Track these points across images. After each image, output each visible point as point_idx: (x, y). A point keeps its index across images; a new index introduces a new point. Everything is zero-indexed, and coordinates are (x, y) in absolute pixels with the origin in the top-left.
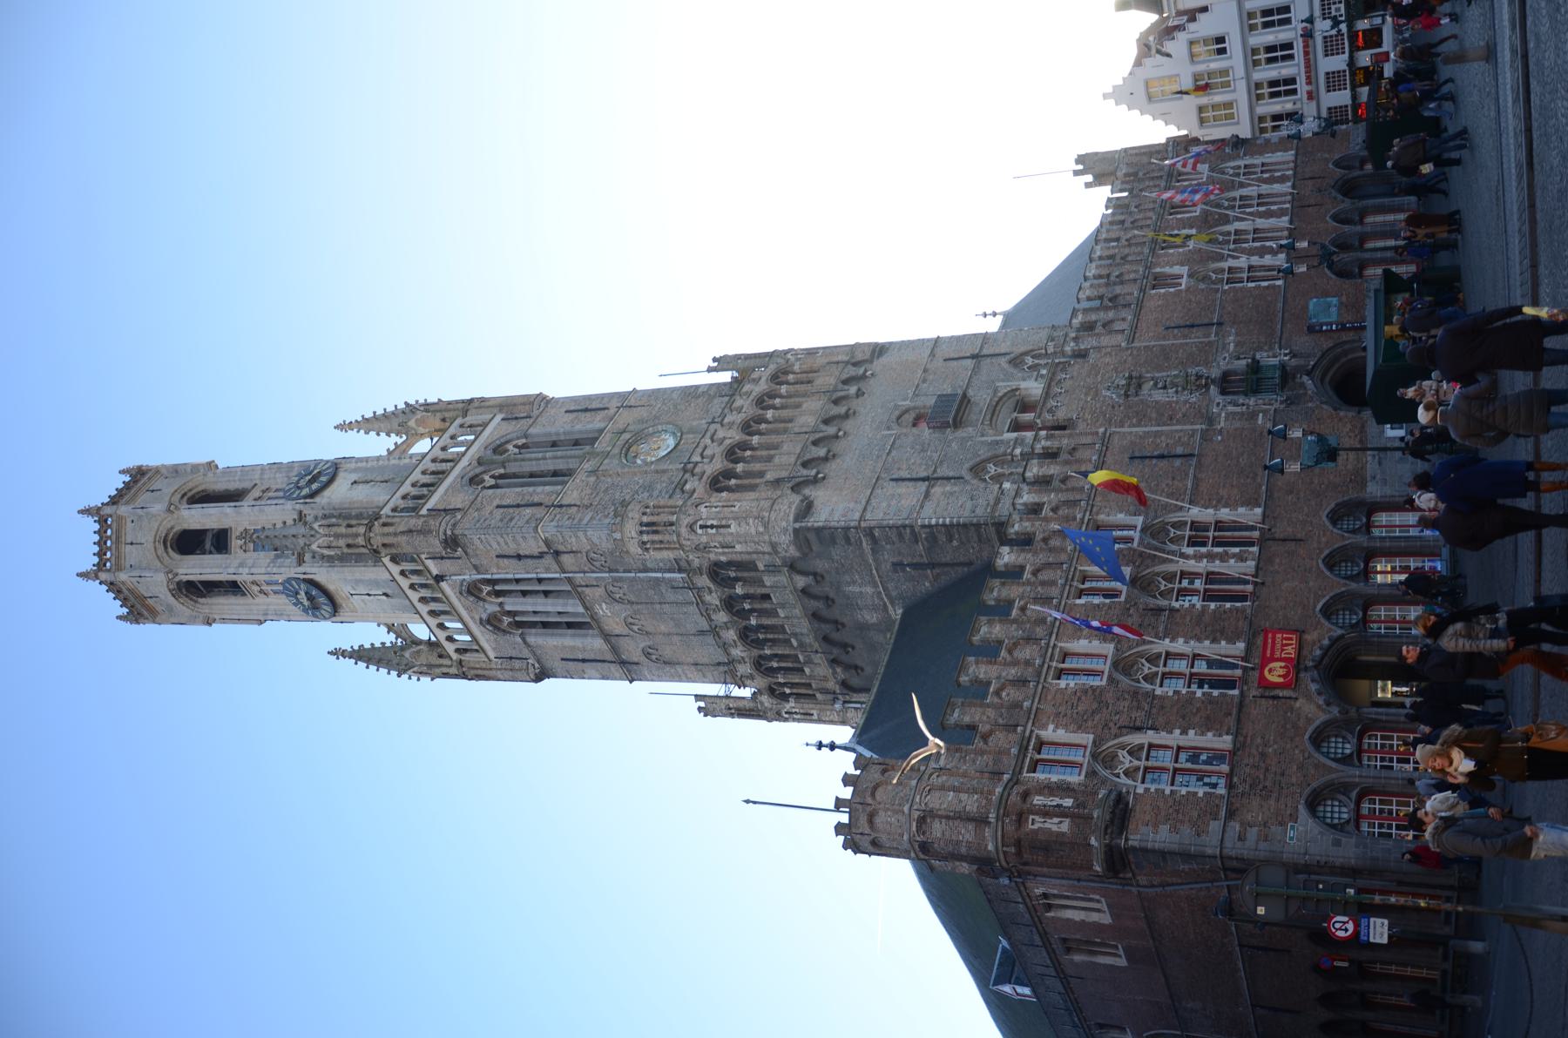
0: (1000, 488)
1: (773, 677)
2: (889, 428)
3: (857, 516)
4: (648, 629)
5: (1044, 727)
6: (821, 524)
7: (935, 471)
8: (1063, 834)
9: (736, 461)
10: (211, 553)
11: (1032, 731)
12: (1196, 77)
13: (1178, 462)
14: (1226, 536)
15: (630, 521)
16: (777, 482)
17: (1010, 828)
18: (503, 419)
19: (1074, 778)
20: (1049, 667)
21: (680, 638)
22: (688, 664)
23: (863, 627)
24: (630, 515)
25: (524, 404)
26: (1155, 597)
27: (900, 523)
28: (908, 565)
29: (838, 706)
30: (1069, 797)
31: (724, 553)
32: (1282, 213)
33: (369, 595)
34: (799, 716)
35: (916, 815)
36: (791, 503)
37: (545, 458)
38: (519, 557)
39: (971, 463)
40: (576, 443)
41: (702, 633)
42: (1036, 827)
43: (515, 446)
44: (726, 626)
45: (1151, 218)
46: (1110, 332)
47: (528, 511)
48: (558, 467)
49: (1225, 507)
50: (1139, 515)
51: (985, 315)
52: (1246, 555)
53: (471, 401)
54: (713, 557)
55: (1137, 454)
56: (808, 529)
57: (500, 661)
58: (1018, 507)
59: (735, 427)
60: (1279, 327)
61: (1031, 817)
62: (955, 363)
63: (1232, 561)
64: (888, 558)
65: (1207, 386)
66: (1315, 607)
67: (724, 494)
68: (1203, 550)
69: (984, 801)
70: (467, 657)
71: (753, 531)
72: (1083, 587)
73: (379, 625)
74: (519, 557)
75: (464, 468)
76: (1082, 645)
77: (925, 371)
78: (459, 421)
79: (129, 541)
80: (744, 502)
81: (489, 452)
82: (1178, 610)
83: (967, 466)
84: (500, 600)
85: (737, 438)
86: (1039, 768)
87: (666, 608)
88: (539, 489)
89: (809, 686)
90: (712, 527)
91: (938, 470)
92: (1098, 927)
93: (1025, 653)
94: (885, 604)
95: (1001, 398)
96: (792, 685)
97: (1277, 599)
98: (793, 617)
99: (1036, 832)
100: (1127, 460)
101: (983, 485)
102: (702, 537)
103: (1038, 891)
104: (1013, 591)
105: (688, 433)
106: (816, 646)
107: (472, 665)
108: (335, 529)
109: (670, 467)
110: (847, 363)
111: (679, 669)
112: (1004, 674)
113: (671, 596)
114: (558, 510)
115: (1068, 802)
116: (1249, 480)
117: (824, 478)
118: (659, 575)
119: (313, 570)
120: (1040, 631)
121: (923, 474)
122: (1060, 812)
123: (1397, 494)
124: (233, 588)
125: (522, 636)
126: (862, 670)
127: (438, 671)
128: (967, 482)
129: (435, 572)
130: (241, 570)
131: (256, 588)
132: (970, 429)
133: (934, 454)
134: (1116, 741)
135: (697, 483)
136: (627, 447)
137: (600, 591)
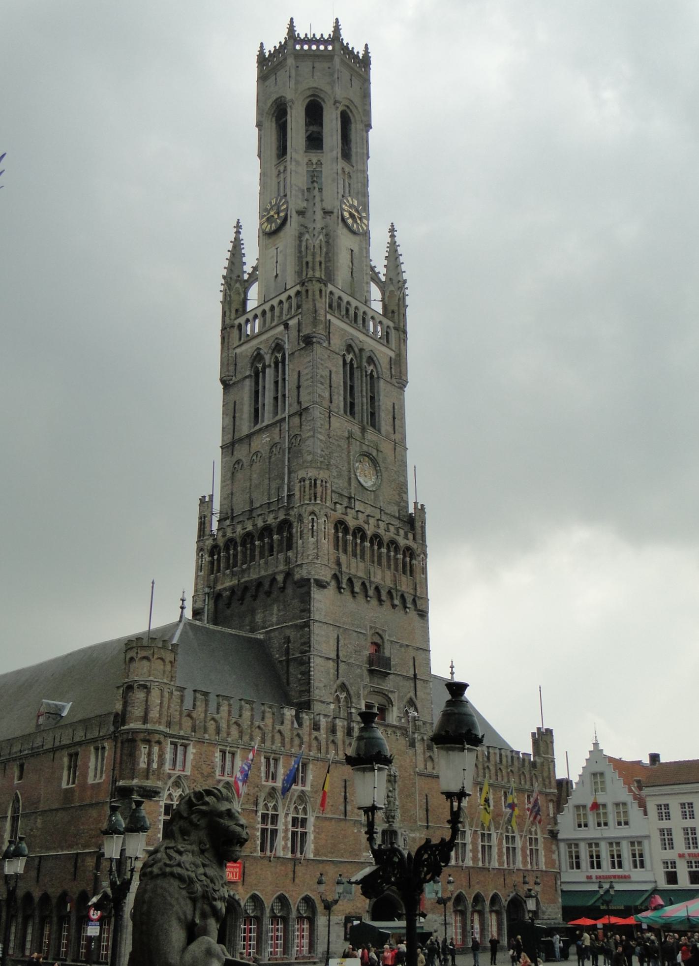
0: (331, 703)
1: (224, 549)
2: (371, 628)
3: (317, 618)
4: (254, 465)
5: (194, 747)
6: (312, 595)
8: (138, 764)
9: (354, 536)
10: (307, 131)
11: (192, 741)
12: (604, 806)
13: (342, 808)
14: (298, 840)
15: (318, 473)
16: (339, 564)
17: (141, 736)
18: (391, 358)
19: (167, 767)
20: (227, 746)
21: (248, 487)
22: (232, 489)
23: (253, 612)
24: (321, 472)
25: (400, 372)
26: (264, 800)
27: (312, 644)
28: (288, 646)
29: (207, 590)
30: (158, 765)
31: (297, 532)
32: (501, 863)
33: (277, 262)
34: (200, 563)
35: (148, 684)
36: (325, 576)
37: (362, 396)
38: (299, 387)
39: (347, 683)
40: (373, 414)
41: (252, 502)
42: (143, 749)
43: (372, 371)
44: (254, 525)
45: (502, 780)
46: (425, 761)
47: (327, 394)
48: (356, 406)
49: (315, 837)
50: (311, 788)
51: (452, 667)
52: (286, 850)
53: (405, 332)
54: (295, 524)
55: (347, 783)
56: (310, 588)
57: (234, 356)
58: (318, 717)
61: (147, 746)
62: (411, 663)
63: (283, 843)
64: (291, 633)
65: (388, 822)
66: (256, 890)
67: (333, 531)
68: (290, 826)
69: (155, 720)
70: (236, 332)
71: (309, 553)
72: (271, 760)
73: (257, 259)
74: (299, 387)
75: (358, 338)
76: (239, 763)
77: (407, 646)
78: (391, 324)
79: (317, 65)
80: (327, 545)
81: (368, 354)
82: (256, 815)
84: (273, 365)
86: (173, 746)
87: (266, 481)
88: (342, 398)
89: (219, 571)
90: (313, 526)
91: (343, 663)
92: (85, 776)
93: (234, 731)
94: (267, 628)
95: (387, 696)
96: (219, 560)
97: (261, 869)
98: (259, 570)
99: (140, 750)
100: (344, 778)
101: (333, 691)
102: (307, 519)
103: (106, 745)
104: (269, 721)
106: (243, 581)
107: (231, 335)
108: (317, 250)
109: (352, 488)
110: (415, 596)
111: (229, 482)
112: (223, 721)
113: (274, 485)
114: (327, 415)
115: (155, 766)
116: (329, 849)
117: (340, 592)
118: (286, 482)
119: (293, 224)
120: (246, 738)
121: (341, 654)
122: (150, 762)
123: (318, 933)
124: (282, 150)
125: (250, 376)
126: (228, 608)
127: (227, 309)
128: (335, 682)
129: (291, 323)
130: (294, 163)
131: (282, 168)
132: (368, 680)
133: (353, 659)
134: (186, 787)
135: (340, 512)
136: (367, 455)
137: (277, 439)
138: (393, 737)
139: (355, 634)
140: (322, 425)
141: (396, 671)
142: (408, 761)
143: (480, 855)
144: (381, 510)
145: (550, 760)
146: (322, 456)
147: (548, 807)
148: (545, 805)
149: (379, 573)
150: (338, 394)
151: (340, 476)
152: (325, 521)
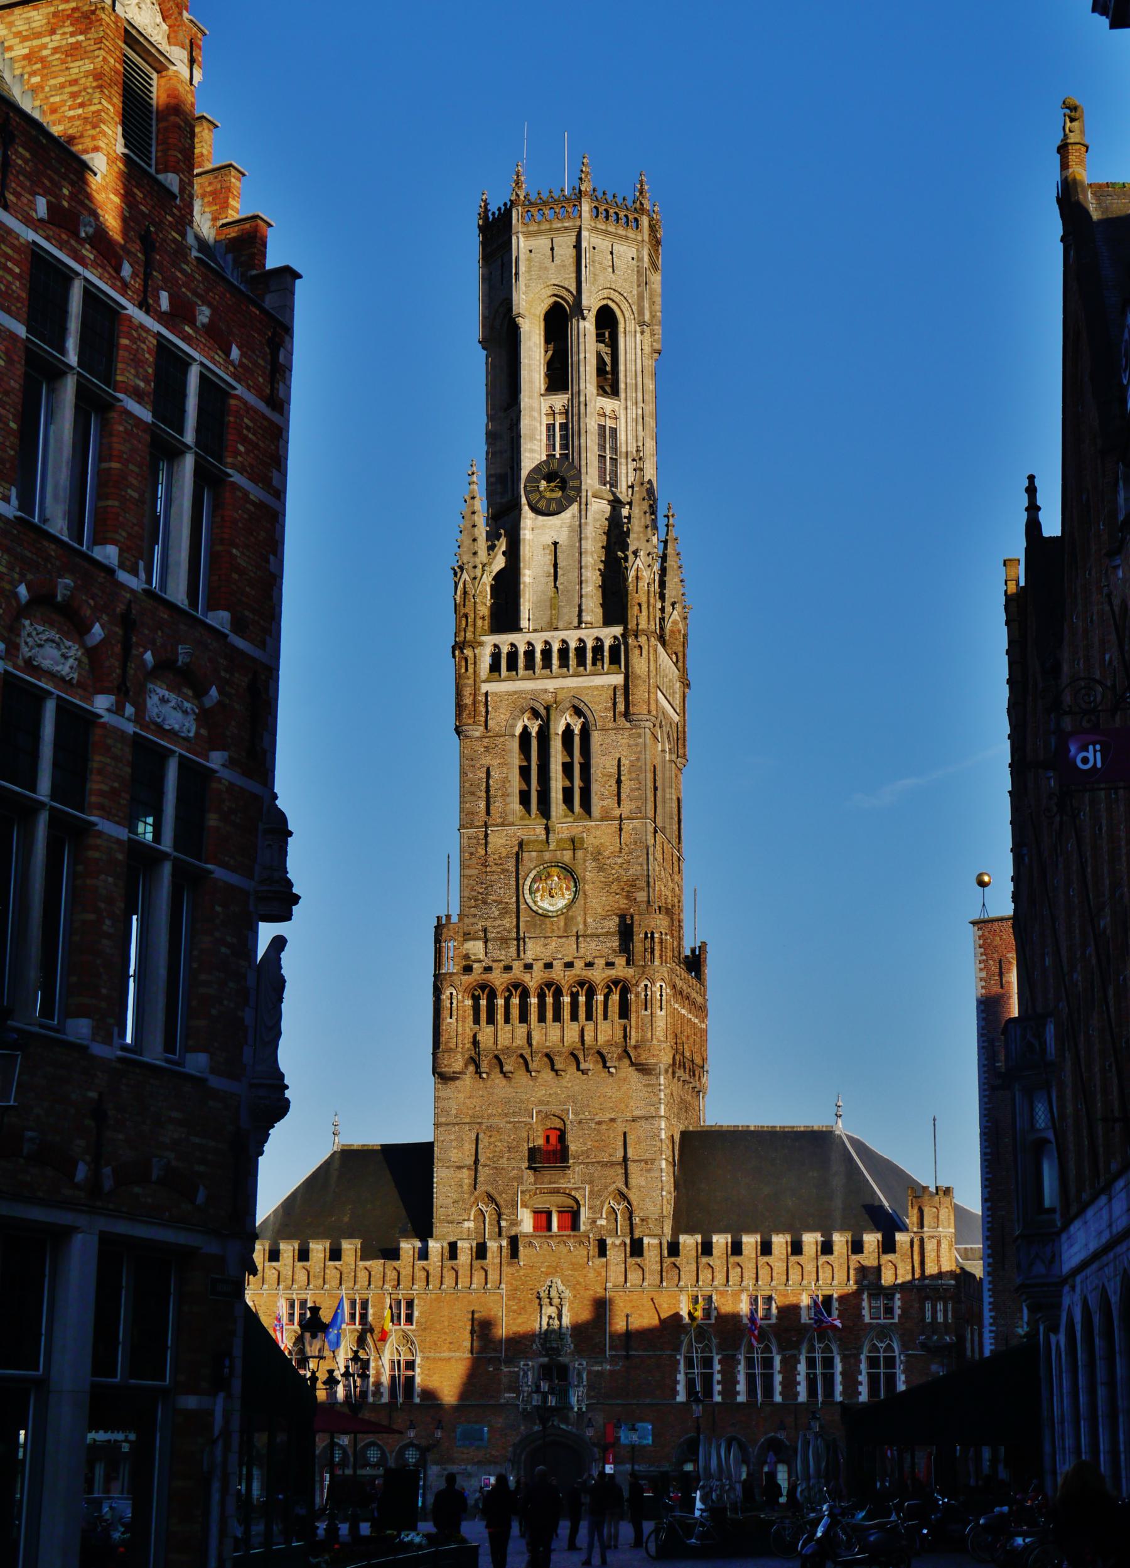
0: (464, 1220)
2: (538, 1112)
7: (485, 1166)
16: (475, 1043)
36: (450, 1066)
47: (482, 805)
59: (546, 975)
60: (619, 1402)
62: (621, 1143)
75: (546, 691)
77: (613, 1120)
81: (568, 705)
83: (490, 1189)
85: (531, 984)
93: (301, 1276)
101: (468, 1206)
105: (566, 919)
112: (288, 1268)
114: (481, 835)
117: (483, 1078)
121: (482, 1159)
133: (505, 1159)
135: (480, 971)
138: (563, 1249)
139: (509, 1126)
140: (471, 854)
141: (588, 1157)
142: (591, 1275)
143: (741, 1387)
144: (578, 937)
145: (925, 1236)
146: (470, 899)
147: (922, 1310)
148: (916, 1305)
149: (553, 1031)
150: (505, 795)
151: (504, 913)
152: (451, 994)
